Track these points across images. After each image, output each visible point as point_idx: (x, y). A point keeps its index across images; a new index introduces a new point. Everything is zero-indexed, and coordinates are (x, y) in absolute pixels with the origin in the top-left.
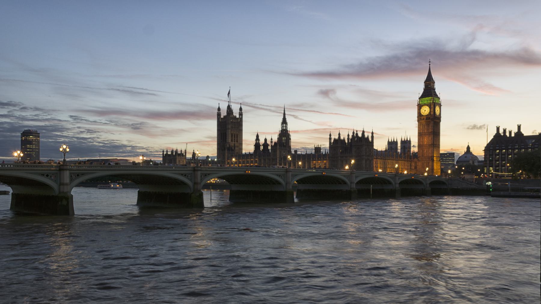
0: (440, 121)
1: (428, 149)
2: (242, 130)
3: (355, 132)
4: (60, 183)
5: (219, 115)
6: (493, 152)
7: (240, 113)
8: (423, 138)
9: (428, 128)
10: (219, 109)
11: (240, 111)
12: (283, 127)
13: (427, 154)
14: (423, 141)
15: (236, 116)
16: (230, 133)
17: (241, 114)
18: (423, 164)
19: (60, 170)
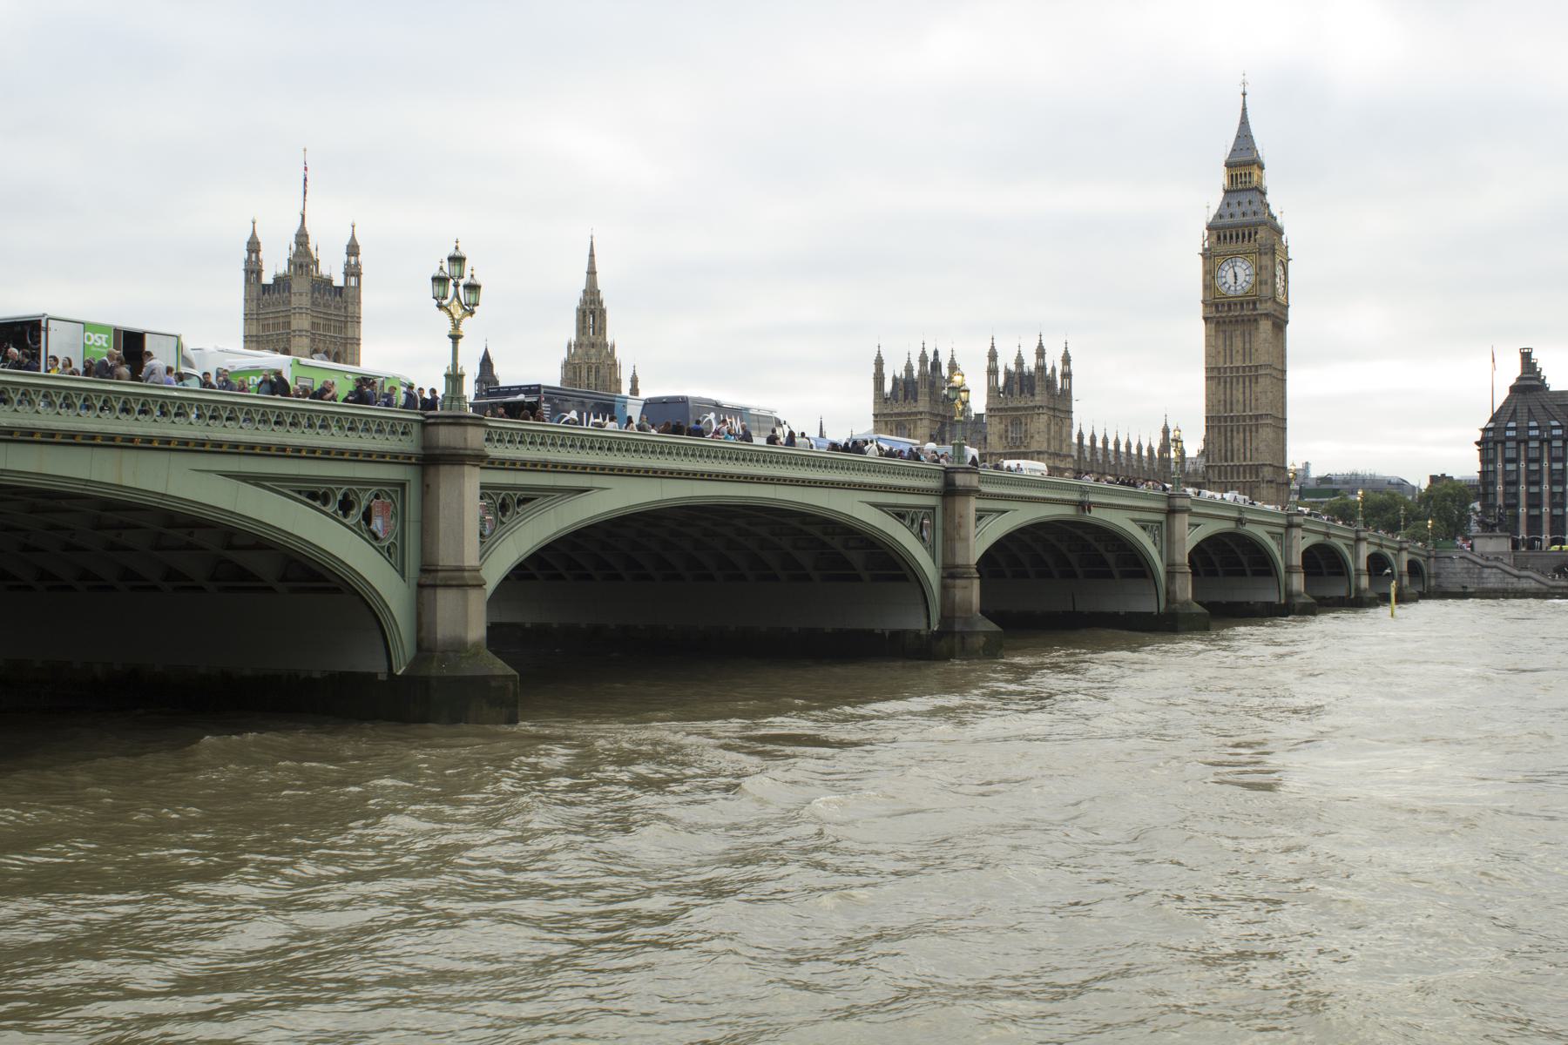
0: (1287, 322)
1: (1248, 434)
2: (359, 339)
3: (931, 358)
4: (427, 568)
5: (252, 272)
6: (1518, 448)
7: (348, 264)
8: (1228, 386)
10: (254, 246)
11: (348, 262)
12: (582, 328)
13: (1244, 453)
14: (1228, 401)
15: (329, 281)
17: (353, 271)
19: (431, 460)
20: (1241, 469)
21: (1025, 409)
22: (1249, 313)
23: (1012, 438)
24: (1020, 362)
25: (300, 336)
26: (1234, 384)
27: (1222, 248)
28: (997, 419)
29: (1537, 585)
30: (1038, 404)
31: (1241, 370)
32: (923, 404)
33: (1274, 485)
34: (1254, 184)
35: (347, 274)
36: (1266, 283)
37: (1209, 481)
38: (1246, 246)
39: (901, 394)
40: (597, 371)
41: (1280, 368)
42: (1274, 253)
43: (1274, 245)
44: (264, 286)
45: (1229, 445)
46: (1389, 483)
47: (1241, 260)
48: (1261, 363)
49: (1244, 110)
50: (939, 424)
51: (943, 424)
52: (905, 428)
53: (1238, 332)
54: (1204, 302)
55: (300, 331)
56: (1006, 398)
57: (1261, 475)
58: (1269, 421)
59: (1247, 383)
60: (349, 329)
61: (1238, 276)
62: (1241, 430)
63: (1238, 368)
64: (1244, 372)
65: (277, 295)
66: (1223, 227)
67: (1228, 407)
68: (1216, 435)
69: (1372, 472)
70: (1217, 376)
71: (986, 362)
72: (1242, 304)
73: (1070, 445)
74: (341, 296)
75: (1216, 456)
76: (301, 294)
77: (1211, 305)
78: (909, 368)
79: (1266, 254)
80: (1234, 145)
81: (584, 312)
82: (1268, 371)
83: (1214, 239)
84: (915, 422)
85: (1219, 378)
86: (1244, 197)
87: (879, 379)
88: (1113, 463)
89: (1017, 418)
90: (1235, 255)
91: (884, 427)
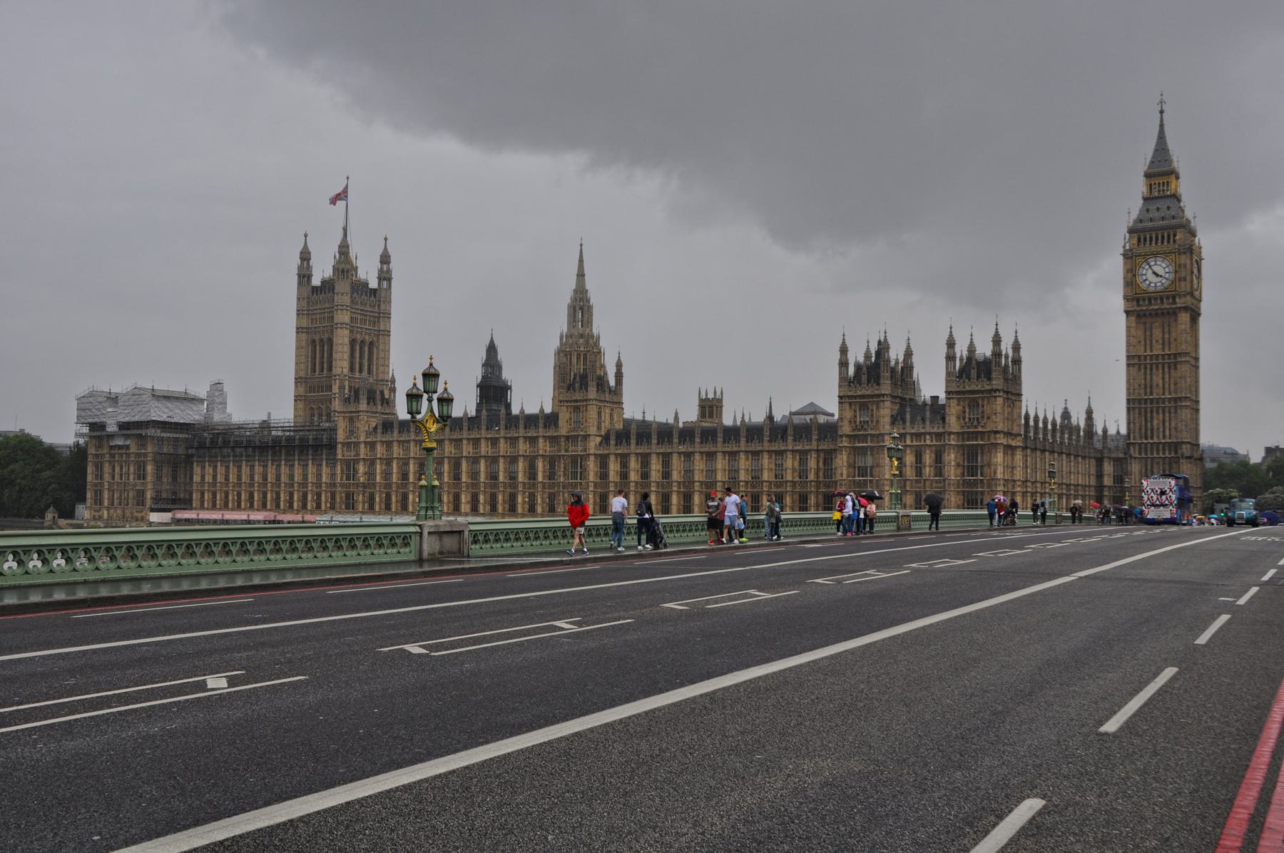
0: (1199, 315)
1: (1167, 415)
7: (381, 271)
8: (1148, 372)
9: (1167, 336)
10: (305, 256)
11: (381, 268)
14: (1148, 385)
15: (367, 284)
16: (347, 340)
17: (385, 276)
18: (1149, 468)
20: (1161, 446)
21: (982, 392)
22: (1168, 307)
23: (970, 419)
24: (972, 349)
25: (341, 328)
26: (1154, 370)
27: (1142, 250)
28: (955, 401)
30: (995, 387)
31: (1160, 357)
32: (886, 388)
33: (1192, 460)
34: (1173, 191)
35: (380, 279)
36: (1185, 280)
37: (1131, 457)
38: (1165, 247)
39: (864, 378)
40: (585, 358)
41: (1193, 355)
42: (1192, 253)
43: (1192, 245)
44: (313, 287)
45: (1149, 424)
46: (1225, 453)
47: (1161, 259)
48: (1179, 351)
49: (1162, 126)
50: (897, 407)
51: (901, 405)
52: (868, 409)
53: (1157, 324)
54: (1126, 298)
55: (341, 324)
56: (964, 382)
57: (1180, 451)
58: (1188, 404)
59: (1166, 370)
60: (382, 323)
61: (1157, 274)
62: (1161, 410)
63: (1157, 355)
64: (1163, 359)
65: (323, 295)
66: (1144, 230)
67: (1148, 390)
68: (1137, 415)
69: (1211, 444)
71: (944, 350)
72: (1162, 299)
73: (1020, 425)
74: (375, 296)
75: (1137, 435)
76: (342, 294)
77: (1133, 300)
78: (867, 356)
79: (1185, 253)
80: (1153, 157)
81: (575, 308)
82: (1187, 358)
83: (1135, 241)
84: (877, 404)
85: (1139, 365)
86: (1163, 204)
87: (843, 364)
88: (1051, 441)
89: (974, 399)
90: (1155, 255)
91: (848, 408)
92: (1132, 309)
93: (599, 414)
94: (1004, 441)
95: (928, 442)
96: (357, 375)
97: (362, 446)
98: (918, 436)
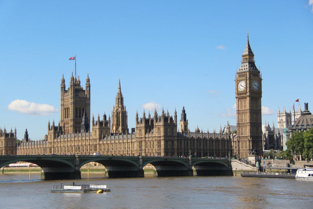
0: (261, 97)
2: (90, 104)
7: (87, 84)
15: (83, 89)
17: (89, 86)
24: (168, 114)
29: (250, 168)
44: (66, 91)
60: (87, 101)
65: (67, 93)
70: (239, 112)
74: (84, 92)
83: (238, 76)
87: (137, 119)
89: (159, 128)
90: (241, 80)
92: (237, 96)
93: (101, 132)
94: (168, 138)
95: (151, 139)
96: (78, 118)
97: (53, 143)
98: (150, 137)
